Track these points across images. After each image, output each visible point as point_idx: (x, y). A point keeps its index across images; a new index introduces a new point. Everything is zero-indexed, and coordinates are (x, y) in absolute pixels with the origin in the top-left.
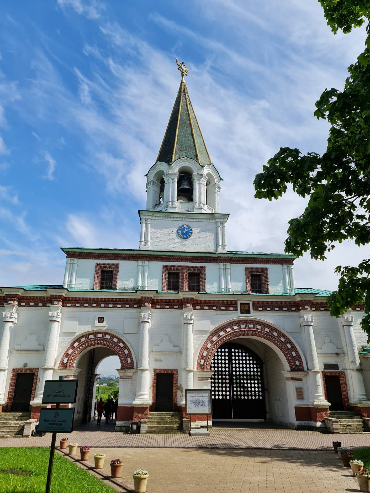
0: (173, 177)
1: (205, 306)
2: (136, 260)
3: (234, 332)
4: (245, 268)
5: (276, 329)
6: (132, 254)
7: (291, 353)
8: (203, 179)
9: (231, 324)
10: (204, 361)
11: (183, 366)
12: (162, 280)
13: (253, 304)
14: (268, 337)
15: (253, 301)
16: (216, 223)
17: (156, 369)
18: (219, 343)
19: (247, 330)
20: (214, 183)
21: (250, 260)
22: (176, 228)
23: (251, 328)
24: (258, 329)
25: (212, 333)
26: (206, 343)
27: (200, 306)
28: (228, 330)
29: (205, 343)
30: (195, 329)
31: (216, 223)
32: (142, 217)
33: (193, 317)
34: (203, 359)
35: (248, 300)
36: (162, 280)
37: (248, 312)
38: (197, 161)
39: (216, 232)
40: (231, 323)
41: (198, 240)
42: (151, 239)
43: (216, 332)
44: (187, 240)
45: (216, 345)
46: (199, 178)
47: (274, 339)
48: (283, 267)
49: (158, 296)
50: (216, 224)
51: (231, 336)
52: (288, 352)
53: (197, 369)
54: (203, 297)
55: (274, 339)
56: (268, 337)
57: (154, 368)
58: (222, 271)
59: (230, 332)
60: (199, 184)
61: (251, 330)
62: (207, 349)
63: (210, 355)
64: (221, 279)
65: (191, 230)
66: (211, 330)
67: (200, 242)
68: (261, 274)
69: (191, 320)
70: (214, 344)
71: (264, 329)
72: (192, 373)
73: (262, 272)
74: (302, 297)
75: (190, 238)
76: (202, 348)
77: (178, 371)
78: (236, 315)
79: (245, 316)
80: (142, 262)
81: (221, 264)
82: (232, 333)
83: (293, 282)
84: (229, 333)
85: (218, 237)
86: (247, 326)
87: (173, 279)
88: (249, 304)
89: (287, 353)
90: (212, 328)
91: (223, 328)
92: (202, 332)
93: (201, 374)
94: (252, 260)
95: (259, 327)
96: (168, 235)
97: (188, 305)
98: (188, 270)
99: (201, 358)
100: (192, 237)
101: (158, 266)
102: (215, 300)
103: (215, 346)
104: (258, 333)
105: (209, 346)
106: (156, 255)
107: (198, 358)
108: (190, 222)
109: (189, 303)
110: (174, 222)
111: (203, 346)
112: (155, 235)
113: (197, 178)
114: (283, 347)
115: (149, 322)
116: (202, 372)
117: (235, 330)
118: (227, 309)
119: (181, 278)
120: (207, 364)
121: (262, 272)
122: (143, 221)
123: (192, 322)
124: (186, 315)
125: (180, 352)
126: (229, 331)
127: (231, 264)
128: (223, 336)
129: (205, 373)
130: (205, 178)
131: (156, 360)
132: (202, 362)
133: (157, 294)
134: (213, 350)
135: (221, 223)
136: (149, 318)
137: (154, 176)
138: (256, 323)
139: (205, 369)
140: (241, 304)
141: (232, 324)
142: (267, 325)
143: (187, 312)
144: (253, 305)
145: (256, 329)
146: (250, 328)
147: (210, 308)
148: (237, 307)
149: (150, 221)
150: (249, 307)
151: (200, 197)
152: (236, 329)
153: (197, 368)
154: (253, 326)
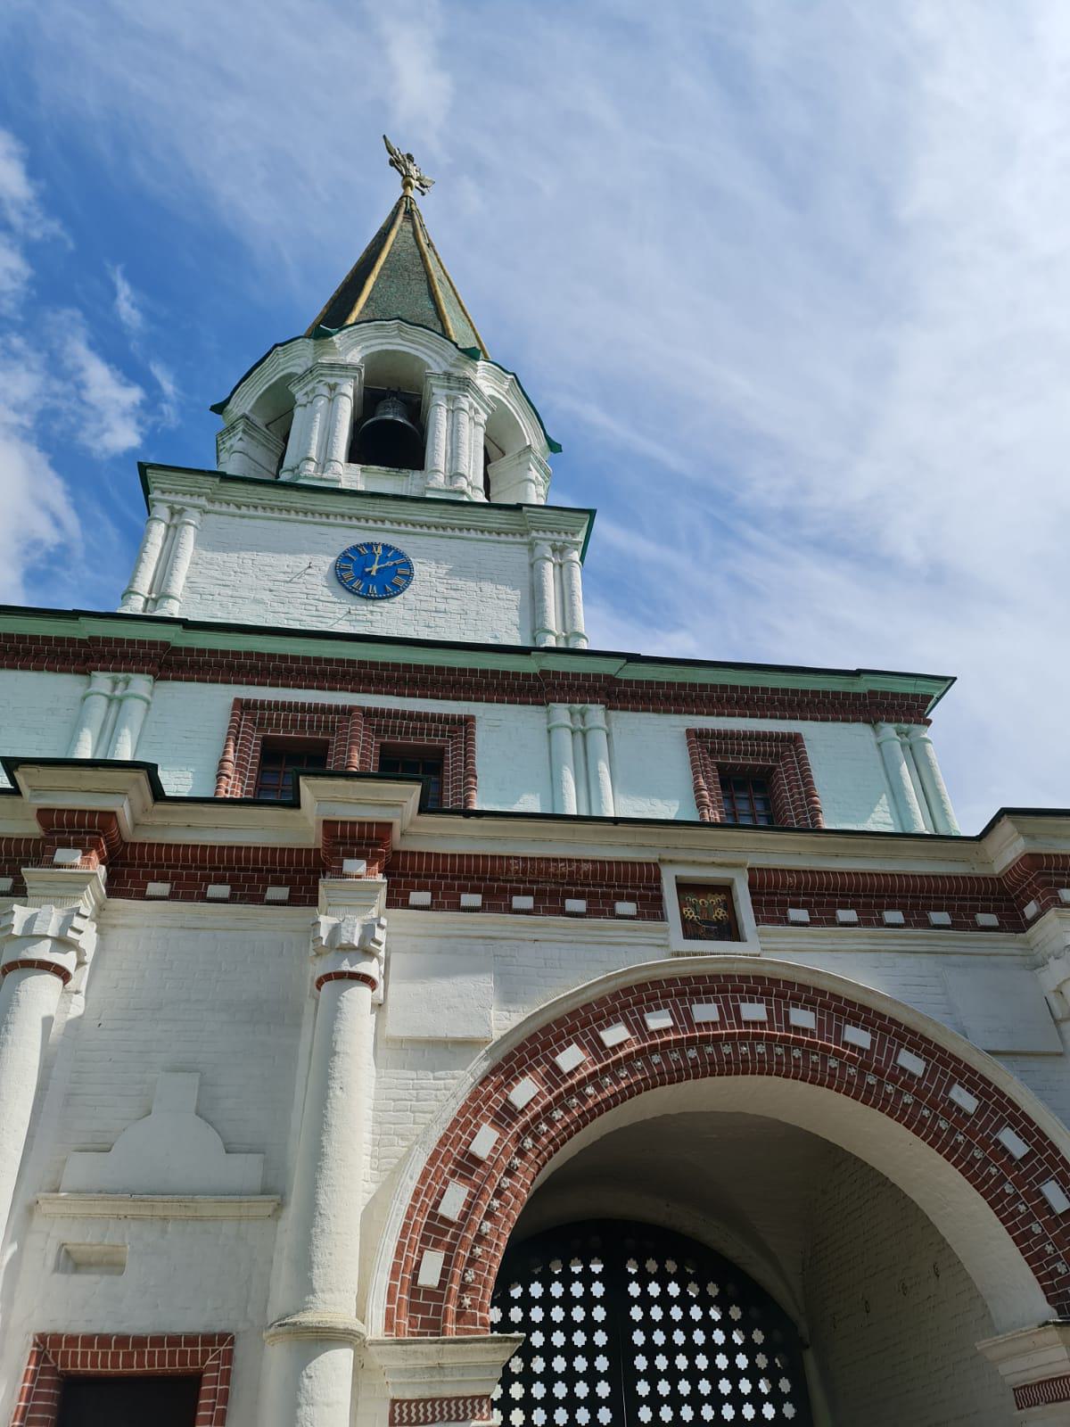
0: (332, 381)
1: (464, 889)
2: (77, 672)
3: (654, 1049)
4: (688, 731)
5: (914, 1033)
6: (60, 641)
7: (1040, 1193)
8: (471, 399)
9: (630, 1000)
10: (447, 1261)
11: (280, 1300)
12: (221, 767)
13: (751, 885)
14: (872, 1080)
15: (751, 870)
16: (532, 546)
17: (56, 1339)
18: (551, 1123)
19: (730, 1037)
20: (522, 447)
21: (710, 699)
22: (331, 556)
23: (755, 1024)
24: (797, 1029)
25: (509, 1058)
26: (464, 1124)
27: (435, 891)
28: (615, 1035)
29: (456, 1121)
30: (392, 1030)
31: (532, 546)
32: (155, 495)
33: (380, 935)
34: (437, 1244)
35: (721, 865)
36: (221, 767)
37: (730, 931)
38: (445, 334)
39: (532, 585)
40: (627, 991)
41: (442, 607)
42: (191, 585)
43: (529, 1051)
44: (385, 605)
45: (536, 1139)
46: (453, 393)
47: (908, 1099)
48: (877, 733)
49: (165, 827)
50: (532, 550)
51: (632, 1072)
52: (1018, 1183)
53: (389, 1325)
54: (452, 837)
55: (908, 1099)
56: (872, 1080)
57: (48, 1328)
58: (565, 740)
59: (627, 1050)
60: (454, 412)
61: (758, 1037)
62: (468, 1165)
63: (489, 1215)
64: (560, 774)
65: (408, 565)
66: (496, 1035)
67: (454, 602)
68: (773, 768)
69: (370, 954)
70: (517, 1128)
71: (839, 1031)
72: (340, 1361)
73: (779, 757)
74: (1031, 837)
75: (397, 599)
76: (432, 1161)
77: (240, 1351)
78: (658, 947)
79: (715, 953)
80: (115, 684)
81: (561, 711)
82: (641, 1052)
83: (942, 802)
84: (621, 1054)
85: (542, 600)
86: (730, 1013)
87: (282, 759)
88: (726, 889)
89: (1009, 1189)
90: (501, 1022)
91: (579, 1022)
92: (442, 1050)
93: (412, 1372)
94: (719, 699)
95: (803, 1018)
96: (282, 577)
97: (356, 866)
98: (378, 732)
99: (425, 1240)
100: (406, 594)
101: (212, 702)
102: (525, 859)
103: (528, 1143)
104: (805, 1053)
105: (485, 1141)
106: (201, 652)
107: (404, 1233)
108: (403, 538)
109: (360, 856)
110: (324, 529)
111: (442, 1143)
112: (216, 574)
113: (446, 391)
114: (978, 1154)
115: (64, 975)
116: (427, 1352)
117: (652, 1034)
118: (601, 906)
119: (338, 753)
120: (465, 1287)
121: (779, 757)
122: (162, 511)
123: (372, 968)
124: (334, 920)
125: (273, 1193)
126: (621, 1046)
127: (613, 714)
128: (578, 1077)
129: (451, 1356)
130: (484, 401)
131: (71, 1262)
132: (431, 1269)
133: (161, 807)
134: (510, 1172)
135: (554, 550)
136: (62, 943)
137: (254, 407)
138: (781, 995)
139: (451, 1326)
140: (684, 887)
141: (638, 1002)
142: (850, 1003)
143: (343, 910)
144: (752, 894)
145: (789, 1028)
146: (747, 1024)
147: (497, 901)
148: (659, 898)
149: (197, 515)
150: (729, 905)
151: (454, 455)
152: (660, 1032)
153: (389, 1313)
154: (769, 1012)
